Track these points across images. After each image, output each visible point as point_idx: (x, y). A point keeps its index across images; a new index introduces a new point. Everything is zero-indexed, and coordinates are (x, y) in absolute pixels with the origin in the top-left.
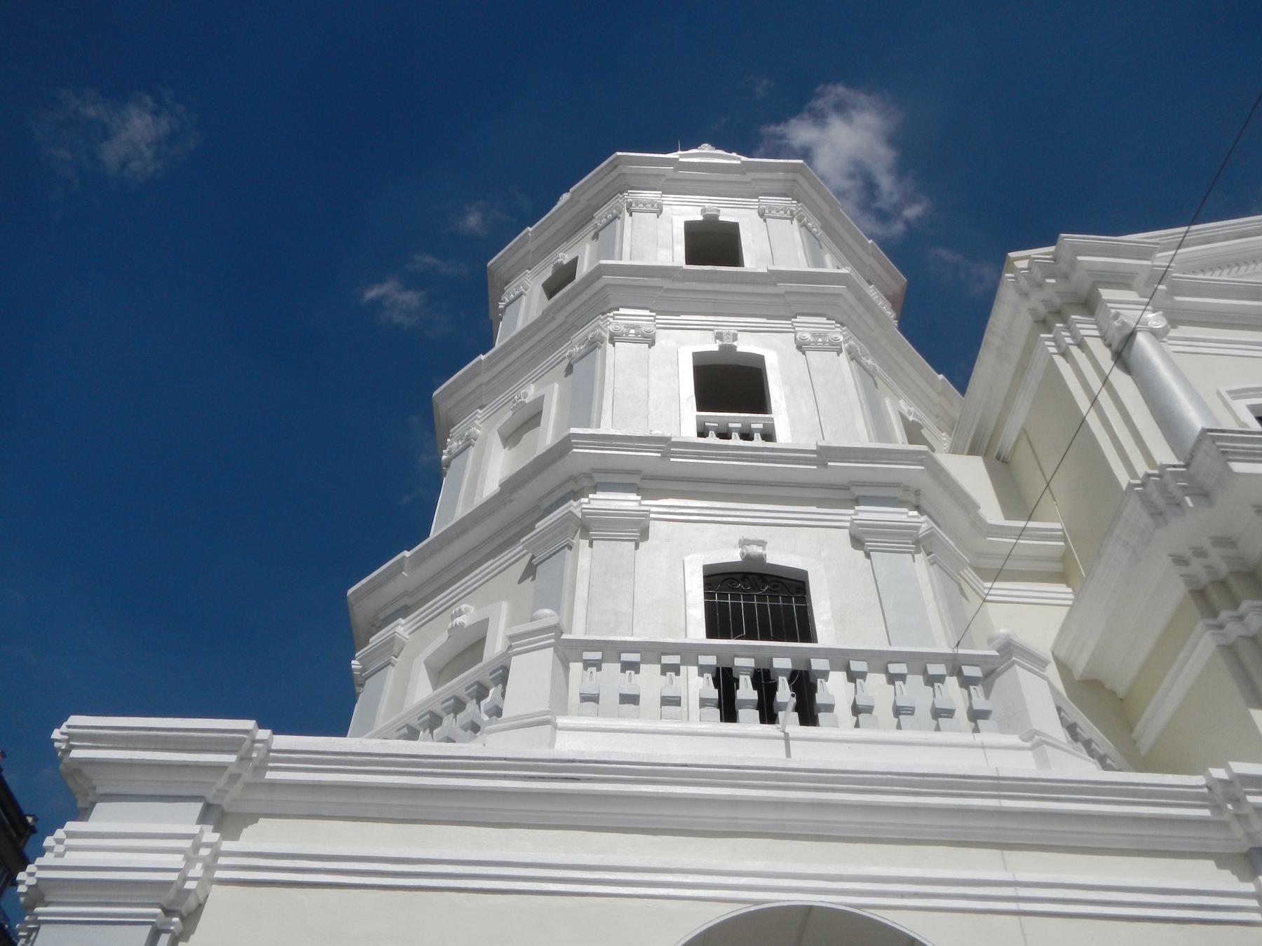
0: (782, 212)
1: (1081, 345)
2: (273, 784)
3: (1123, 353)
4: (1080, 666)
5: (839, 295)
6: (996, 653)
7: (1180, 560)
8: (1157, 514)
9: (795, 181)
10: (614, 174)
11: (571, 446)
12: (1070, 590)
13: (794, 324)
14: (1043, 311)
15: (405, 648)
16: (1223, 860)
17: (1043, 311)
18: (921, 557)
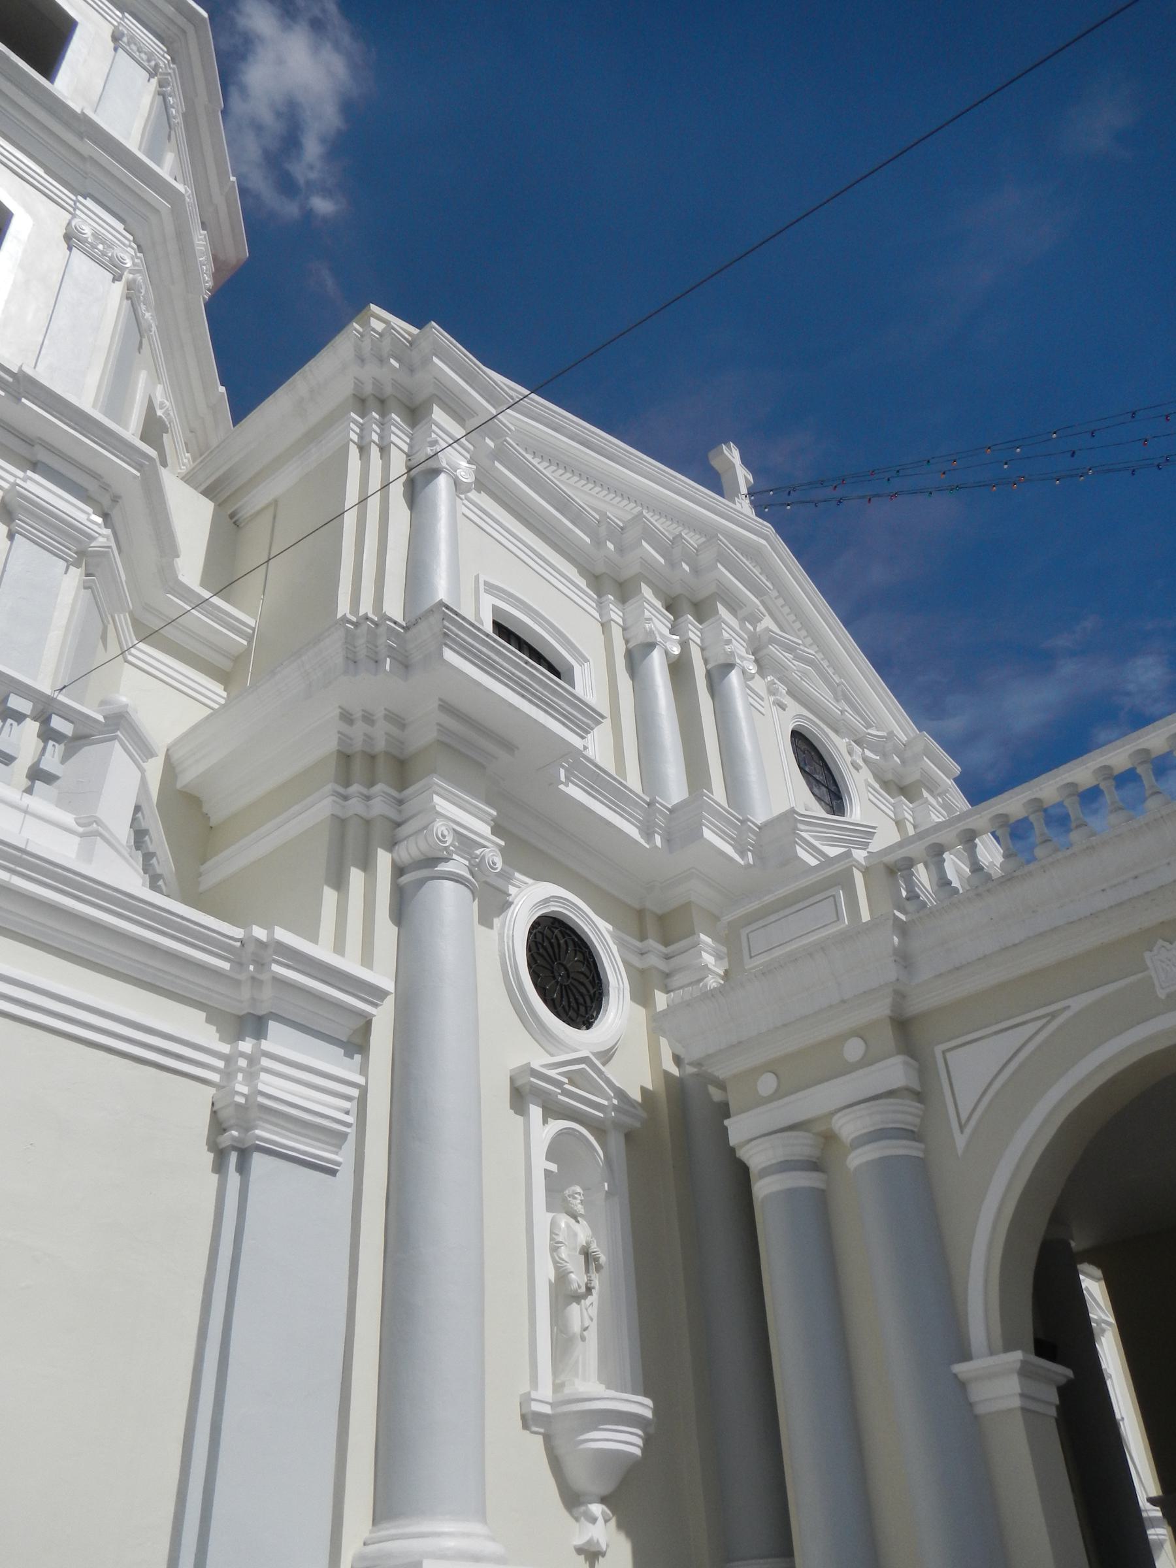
1: (384, 450)
4: (187, 777)
5: (156, 211)
6: (101, 719)
7: (346, 717)
8: (352, 661)
12: (225, 694)
13: (78, 204)
14: (368, 389)
16: (214, 1016)
17: (368, 389)
18: (76, 573)
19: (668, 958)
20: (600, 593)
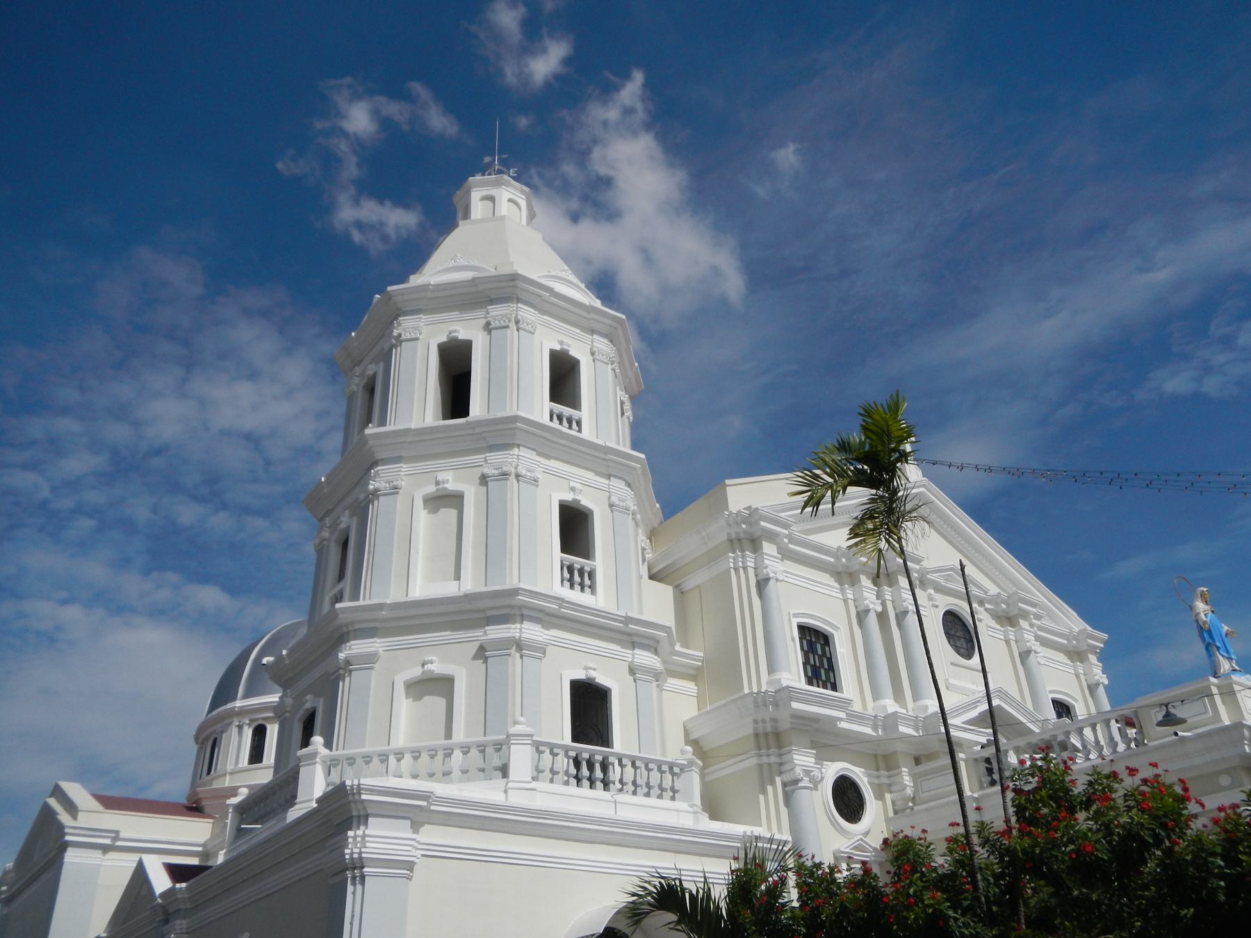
0: (605, 357)
2: (433, 811)
3: (762, 584)
5: (634, 468)
7: (756, 722)
9: (616, 328)
10: (511, 284)
11: (518, 594)
12: (696, 688)
14: (734, 536)
15: (380, 659)
17: (734, 536)
19: (889, 777)
20: (841, 584)
